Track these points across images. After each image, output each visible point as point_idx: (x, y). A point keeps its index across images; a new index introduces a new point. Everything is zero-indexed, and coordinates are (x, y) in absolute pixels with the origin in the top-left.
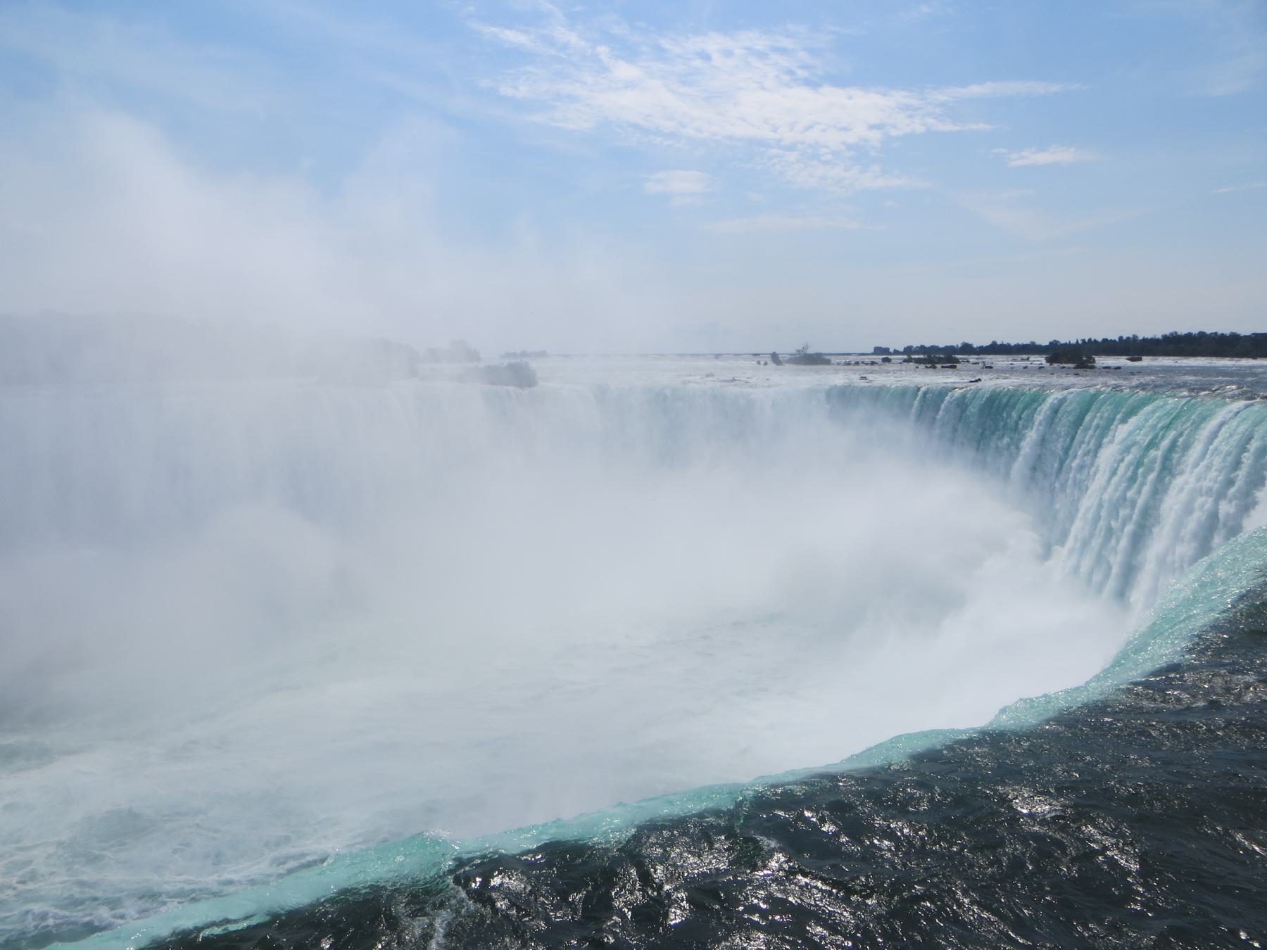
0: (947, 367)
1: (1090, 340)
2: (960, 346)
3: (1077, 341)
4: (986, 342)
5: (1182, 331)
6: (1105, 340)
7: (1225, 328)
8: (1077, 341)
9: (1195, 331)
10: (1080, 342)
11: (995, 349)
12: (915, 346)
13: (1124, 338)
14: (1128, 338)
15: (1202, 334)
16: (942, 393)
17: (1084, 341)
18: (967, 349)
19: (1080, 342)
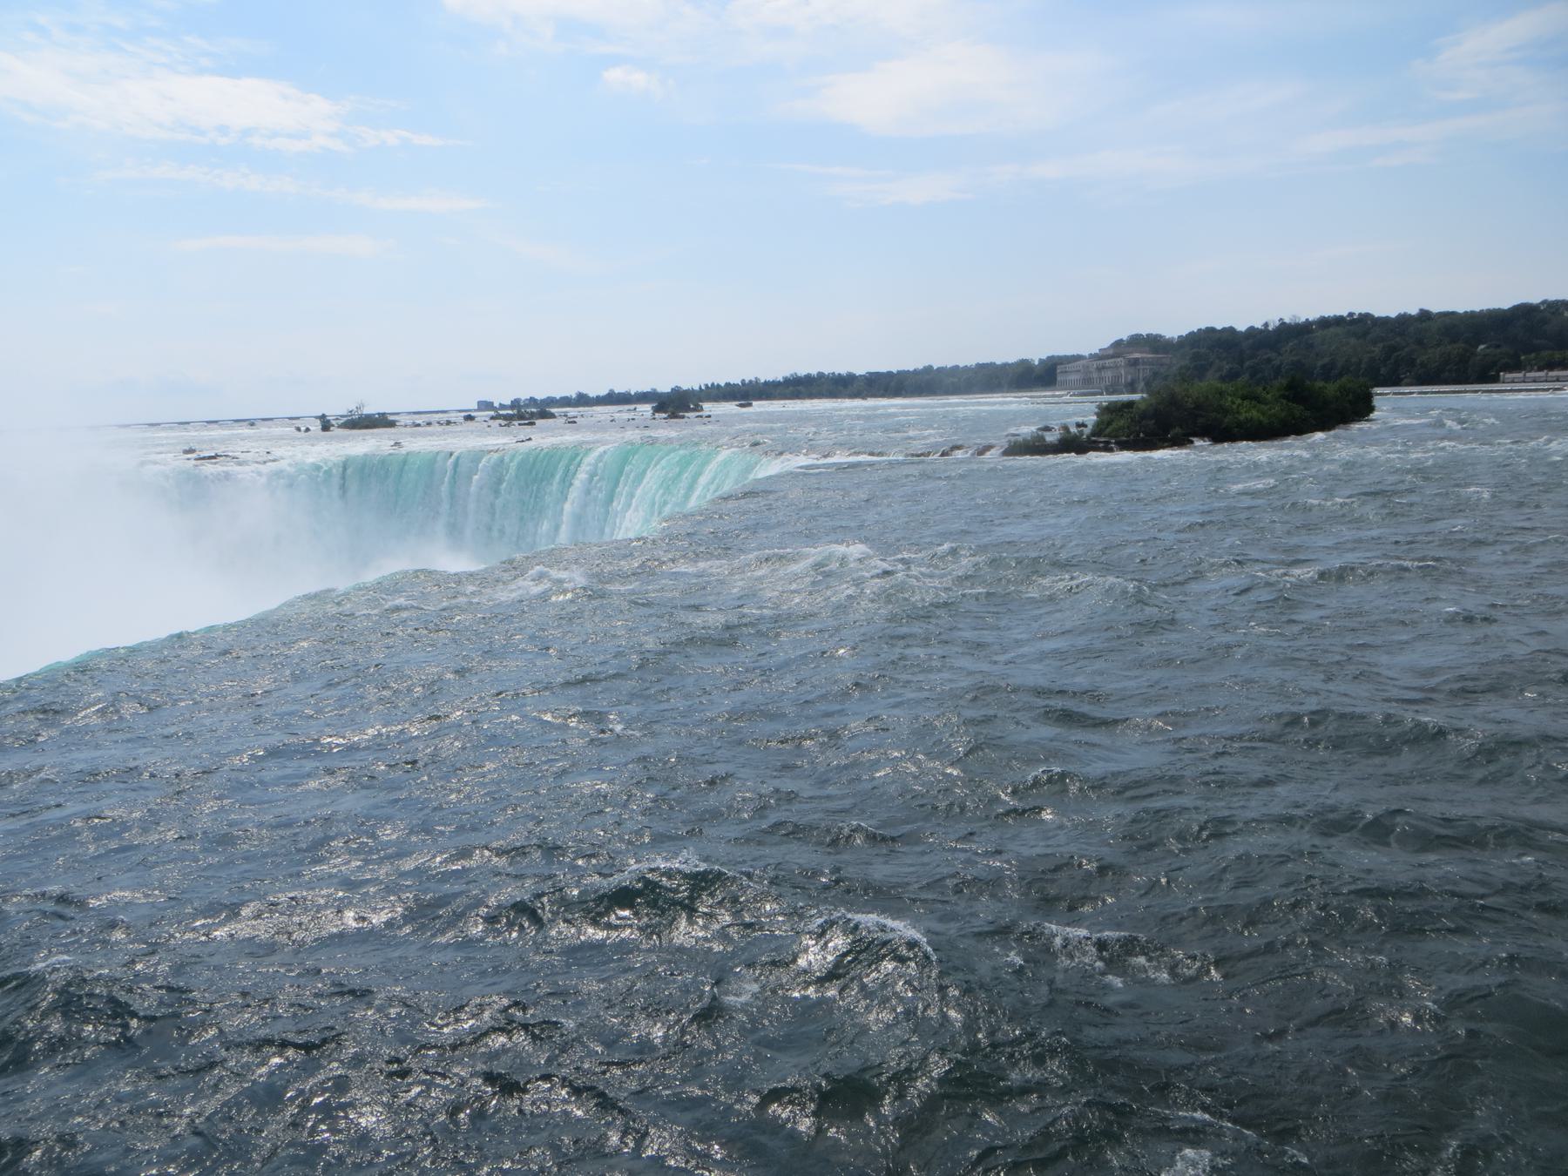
0: (525, 424)
1: (713, 384)
2: (574, 396)
3: (700, 388)
4: (603, 392)
5: (802, 372)
6: (728, 385)
7: (842, 369)
8: (700, 388)
9: (814, 372)
10: (703, 388)
11: (613, 399)
12: (523, 399)
13: (747, 381)
14: (751, 381)
15: (821, 375)
16: (477, 456)
17: (706, 386)
18: (583, 400)
19: (703, 388)
